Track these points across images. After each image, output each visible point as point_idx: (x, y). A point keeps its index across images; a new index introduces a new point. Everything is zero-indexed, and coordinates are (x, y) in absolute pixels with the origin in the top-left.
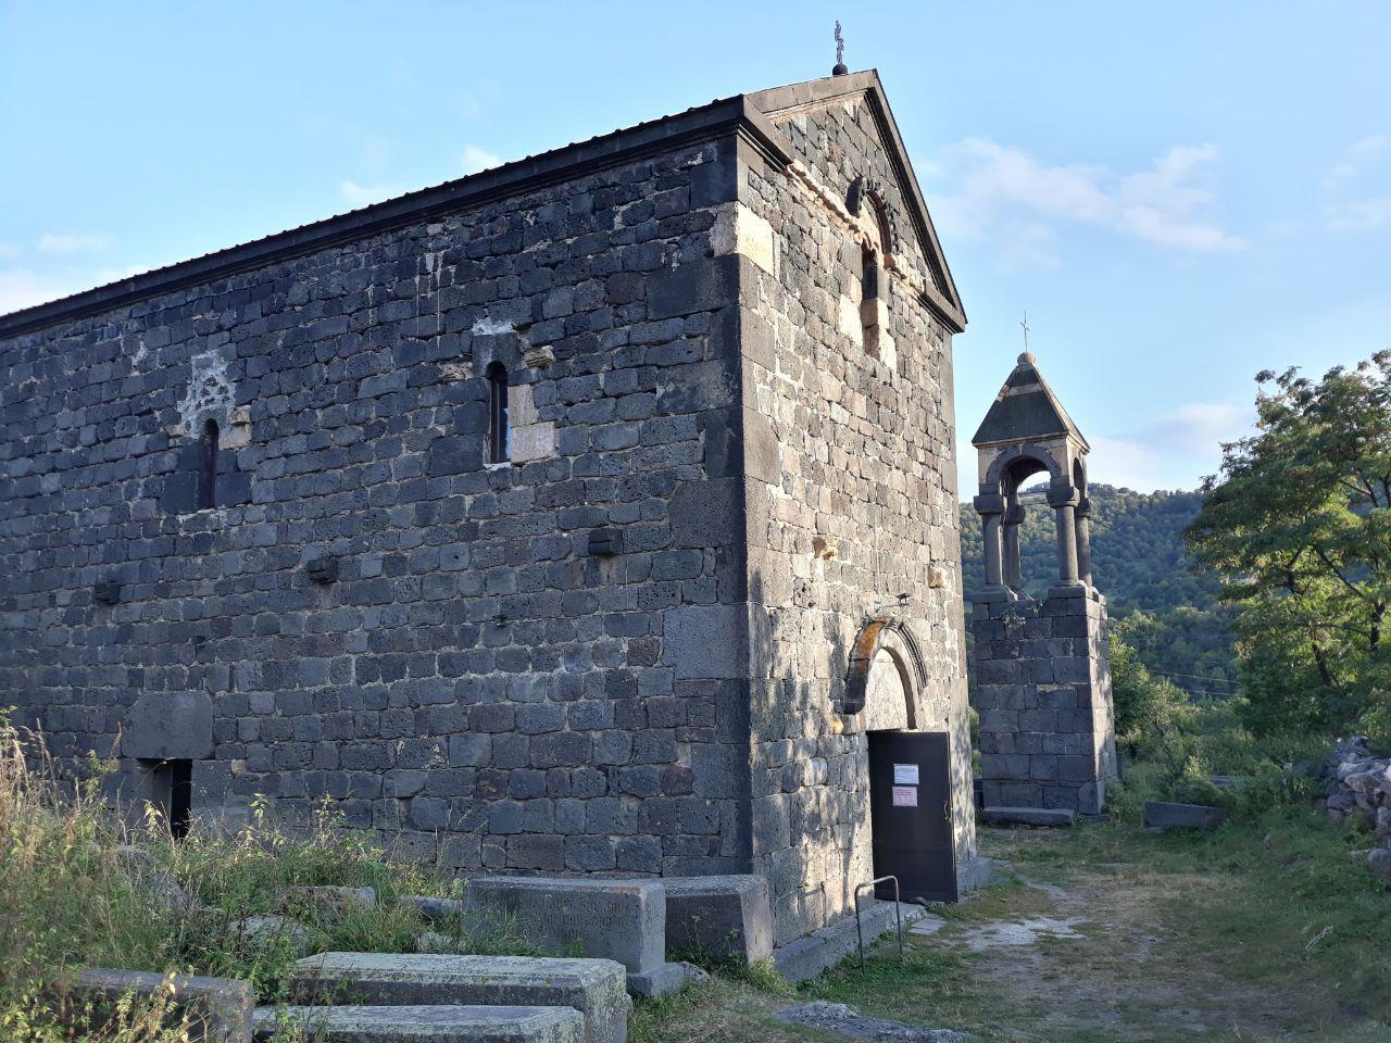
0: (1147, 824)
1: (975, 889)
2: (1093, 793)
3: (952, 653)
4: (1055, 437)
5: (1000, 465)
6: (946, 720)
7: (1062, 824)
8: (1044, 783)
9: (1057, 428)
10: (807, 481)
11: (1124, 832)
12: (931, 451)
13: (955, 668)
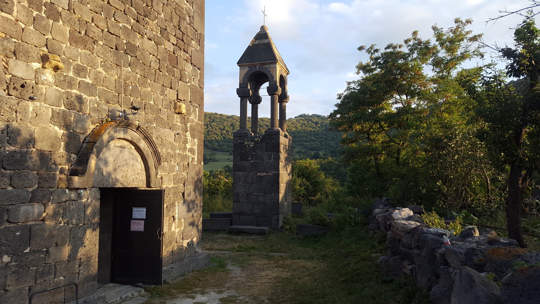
0: (297, 234)
1: (193, 271)
2: (278, 220)
3: (192, 151)
5: (248, 75)
6: (184, 184)
7: (262, 233)
8: (257, 215)
9: (272, 59)
10: (35, 13)
11: (288, 237)
12: (183, 41)
13: (193, 159)
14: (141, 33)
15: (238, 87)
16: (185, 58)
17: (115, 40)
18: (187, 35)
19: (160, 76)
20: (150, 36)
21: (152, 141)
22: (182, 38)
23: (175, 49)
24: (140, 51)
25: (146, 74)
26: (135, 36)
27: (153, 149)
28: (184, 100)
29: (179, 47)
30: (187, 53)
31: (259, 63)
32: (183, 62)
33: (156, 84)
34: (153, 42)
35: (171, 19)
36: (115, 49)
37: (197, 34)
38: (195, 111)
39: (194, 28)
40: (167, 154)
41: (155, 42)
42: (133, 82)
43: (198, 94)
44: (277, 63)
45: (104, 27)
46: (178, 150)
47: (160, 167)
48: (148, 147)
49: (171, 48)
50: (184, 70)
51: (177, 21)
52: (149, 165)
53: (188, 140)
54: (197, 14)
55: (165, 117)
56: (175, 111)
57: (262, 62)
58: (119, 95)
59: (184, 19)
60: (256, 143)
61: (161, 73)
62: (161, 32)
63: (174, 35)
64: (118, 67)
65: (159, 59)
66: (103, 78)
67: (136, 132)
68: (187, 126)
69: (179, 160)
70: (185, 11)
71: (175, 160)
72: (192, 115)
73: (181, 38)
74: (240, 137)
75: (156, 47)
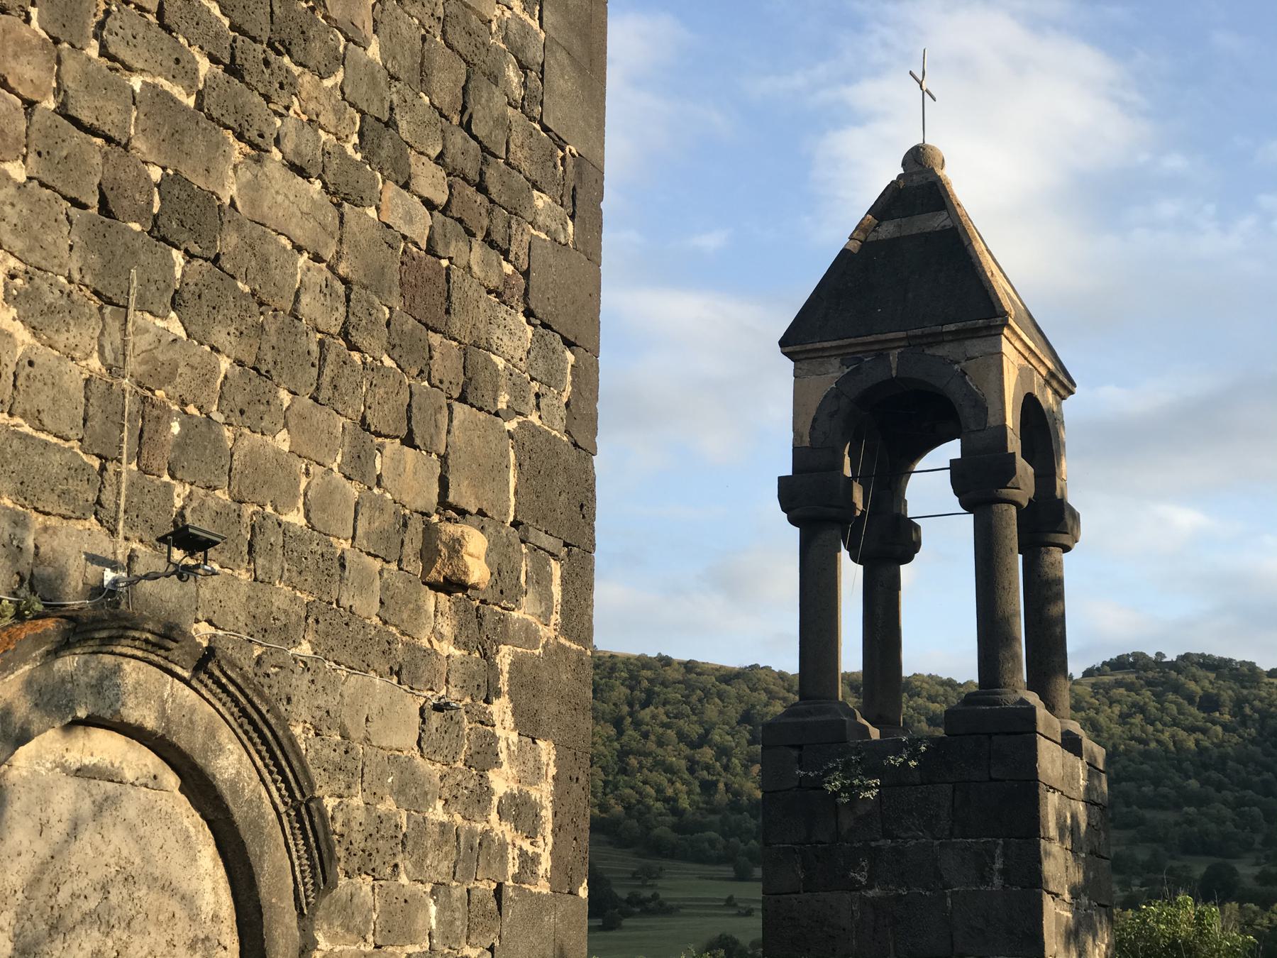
4: (975, 333)
12: (482, 188)
13: (529, 862)
14: (253, 135)
15: (790, 473)
16: (494, 282)
17: (98, 159)
18: (508, 163)
19: (347, 370)
20: (298, 153)
21: (285, 742)
22: (482, 173)
23: (438, 230)
24: (240, 227)
25: (269, 358)
26: (218, 146)
27: (289, 789)
28: (481, 513)
29: (460, 221)
30: (505, 254)
31: (902, 334)
32: (482, 305)
33: (320, 414)
34: (318, 184)
35: (423, 75)
36: (94, 211)
37: (563, 159)
38: (541, 579)
39: (546, 129)
40: (372, 829)
41: (325, 186)
42: (189, 397)
43: (561, 480)
44: (1006, 331)
45: (37, 88)
46: (440, 804)
47: (325, 902)
48: (262, 780)
49: (420, 226)
50: (483, 343)
51: (456, 82)
52: (263, 891)
53: (502, 745)
54: (562, 56)
55: (368, 607)
56: (426, 571)
57: (918, 332)
58: (103, 468)
59: (494, 78)
60: (894, 781)
61: (356, 356)
62: (361, 134)
63: (434, 153)
64: (108, 309)
65: (345, 281)
66: (12, 368)
67: (194, 683)
68: (492, 666)
69: (445, 866)
70: (501, 35)
71: (419, 864)
72: (524, 600)
73: (473, 175)
74: (800, 747)
75: (331, 216)
